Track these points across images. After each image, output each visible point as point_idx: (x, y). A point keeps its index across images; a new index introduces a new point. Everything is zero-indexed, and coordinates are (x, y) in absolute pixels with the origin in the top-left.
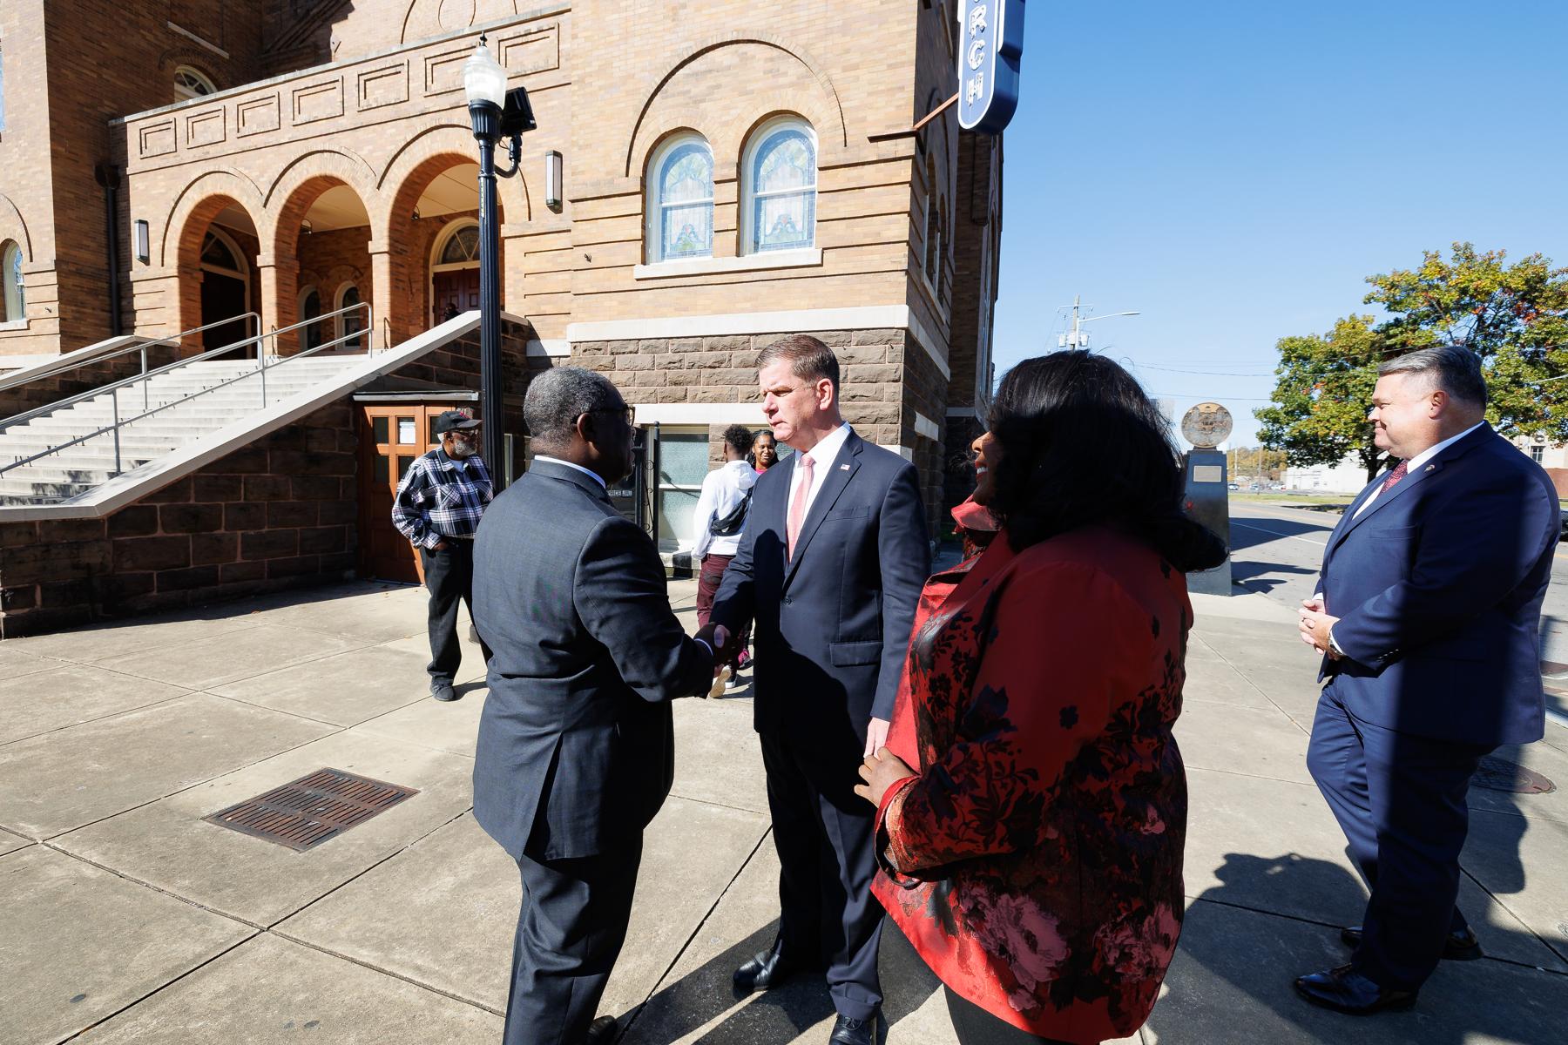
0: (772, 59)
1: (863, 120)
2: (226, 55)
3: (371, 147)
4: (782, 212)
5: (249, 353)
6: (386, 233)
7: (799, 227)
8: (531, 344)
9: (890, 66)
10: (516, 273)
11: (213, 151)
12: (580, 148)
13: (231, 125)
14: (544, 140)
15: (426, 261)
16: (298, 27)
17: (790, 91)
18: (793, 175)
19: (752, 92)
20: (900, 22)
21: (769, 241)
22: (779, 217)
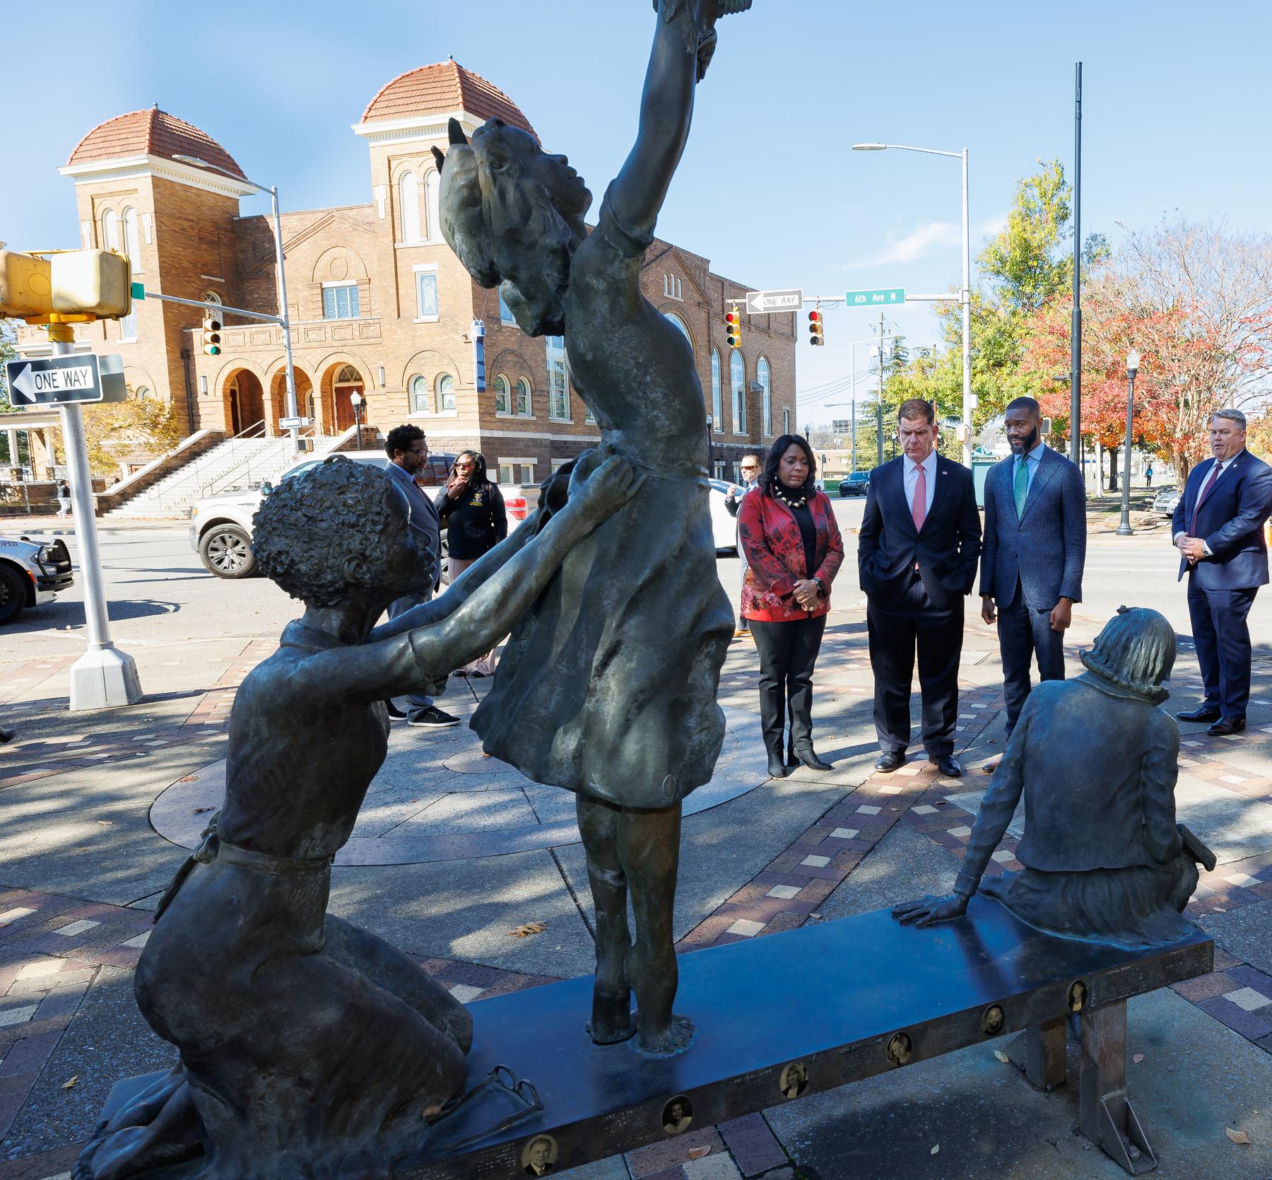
5: (263, 435)
6: (319, 390)
8: (378, 434)
13: (247, 340)
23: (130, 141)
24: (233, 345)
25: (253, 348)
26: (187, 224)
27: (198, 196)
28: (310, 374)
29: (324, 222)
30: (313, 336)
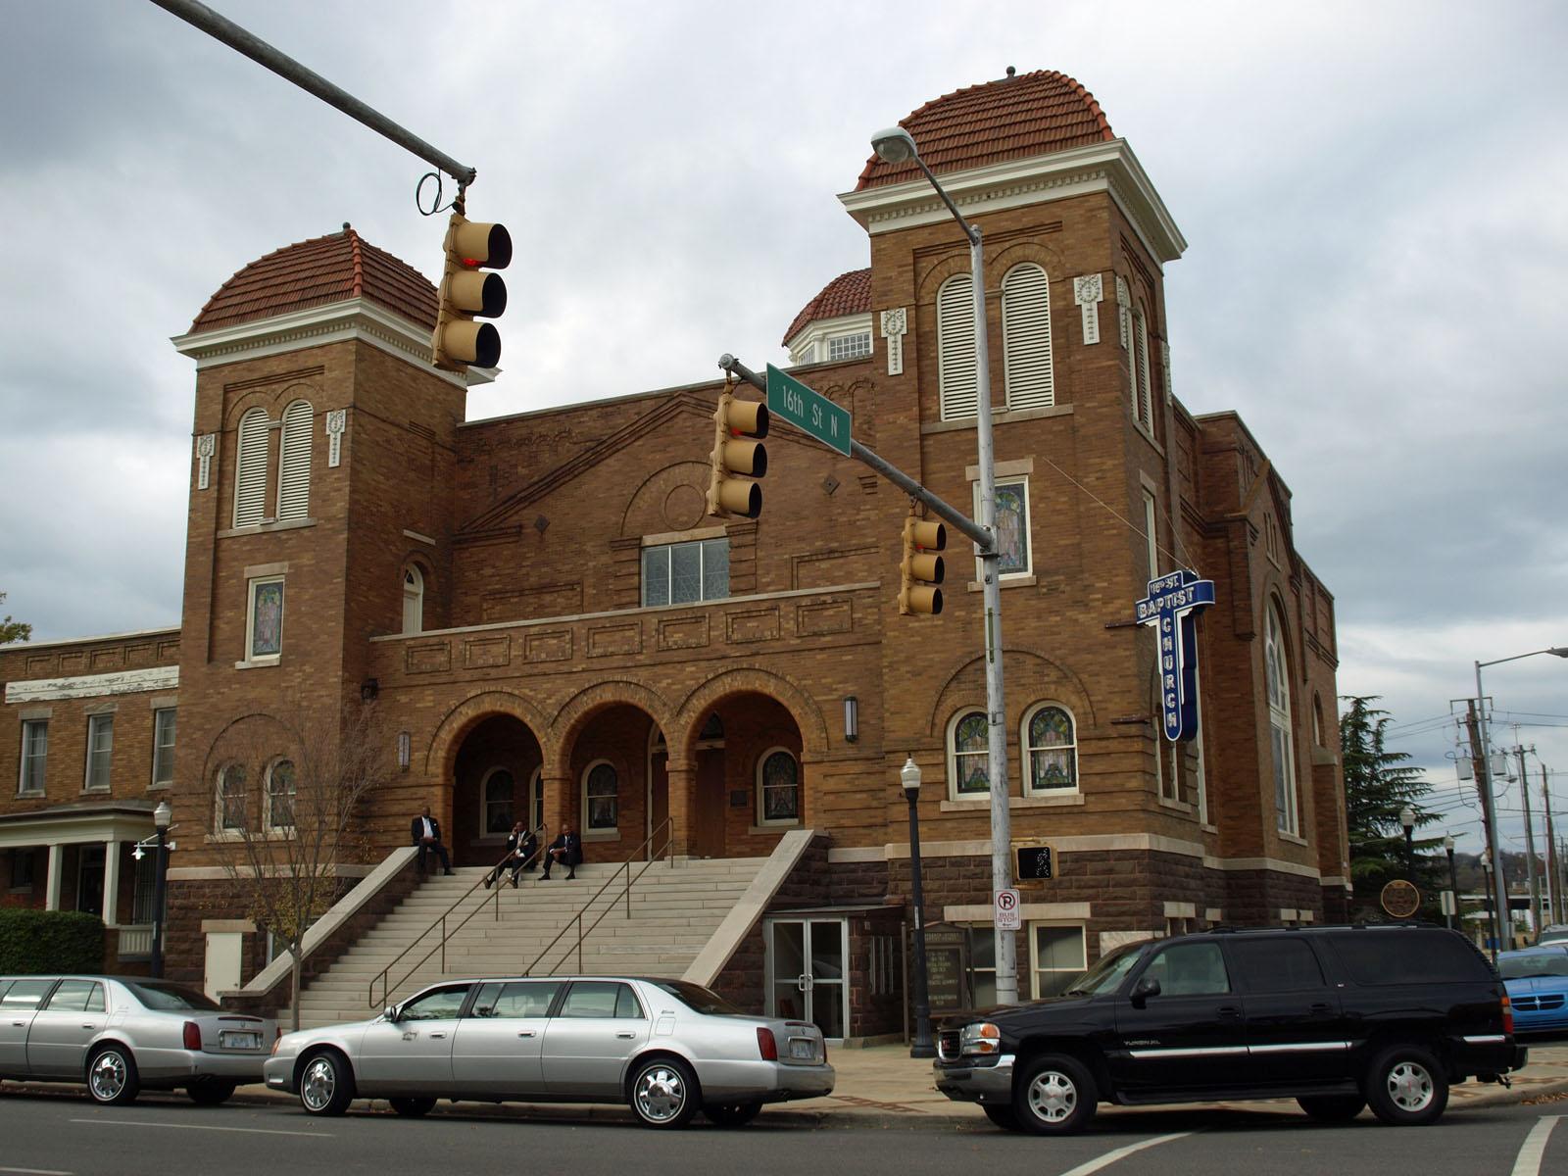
0: (1038, 665)
1: (1106, 709)
2: (432, 542)
3: (670, 681)
4: (1051, 762)
7: (1065, 773)
9: (1121, 677)
10: (816, 792)
11: (494, 673)
12: (892, 714)
14: (841, 686)
15: (646, 742)
16: (502, 508)
17: (1053, 687)
18: (1058, 738)
19: (1023, 685)
20: (1125, 649)
21: (1043, 782)
22: (1050, 765)
23: (320, 281)
24: (480, 662)
25: (527, 669)
26: (395, 431)
27: (414, 379)
28: (663, 720)
29: (658, 417)
30: (678, 636)
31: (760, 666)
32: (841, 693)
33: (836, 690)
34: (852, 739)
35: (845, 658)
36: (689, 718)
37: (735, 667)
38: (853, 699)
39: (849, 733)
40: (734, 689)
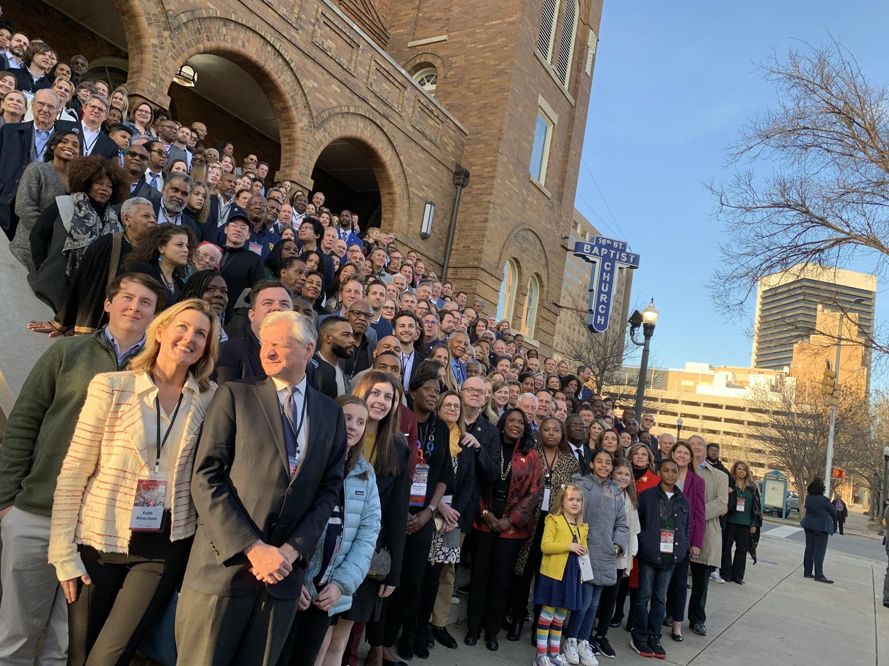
31: (388, 130)
32: (425, 195)
33: (423, 190)
34: (424, 237)
35: (433, 168)
36: (323, 139)
37: (367, 116)
38: (431, 203)
39: (424, 230)
40: (363, 138)
